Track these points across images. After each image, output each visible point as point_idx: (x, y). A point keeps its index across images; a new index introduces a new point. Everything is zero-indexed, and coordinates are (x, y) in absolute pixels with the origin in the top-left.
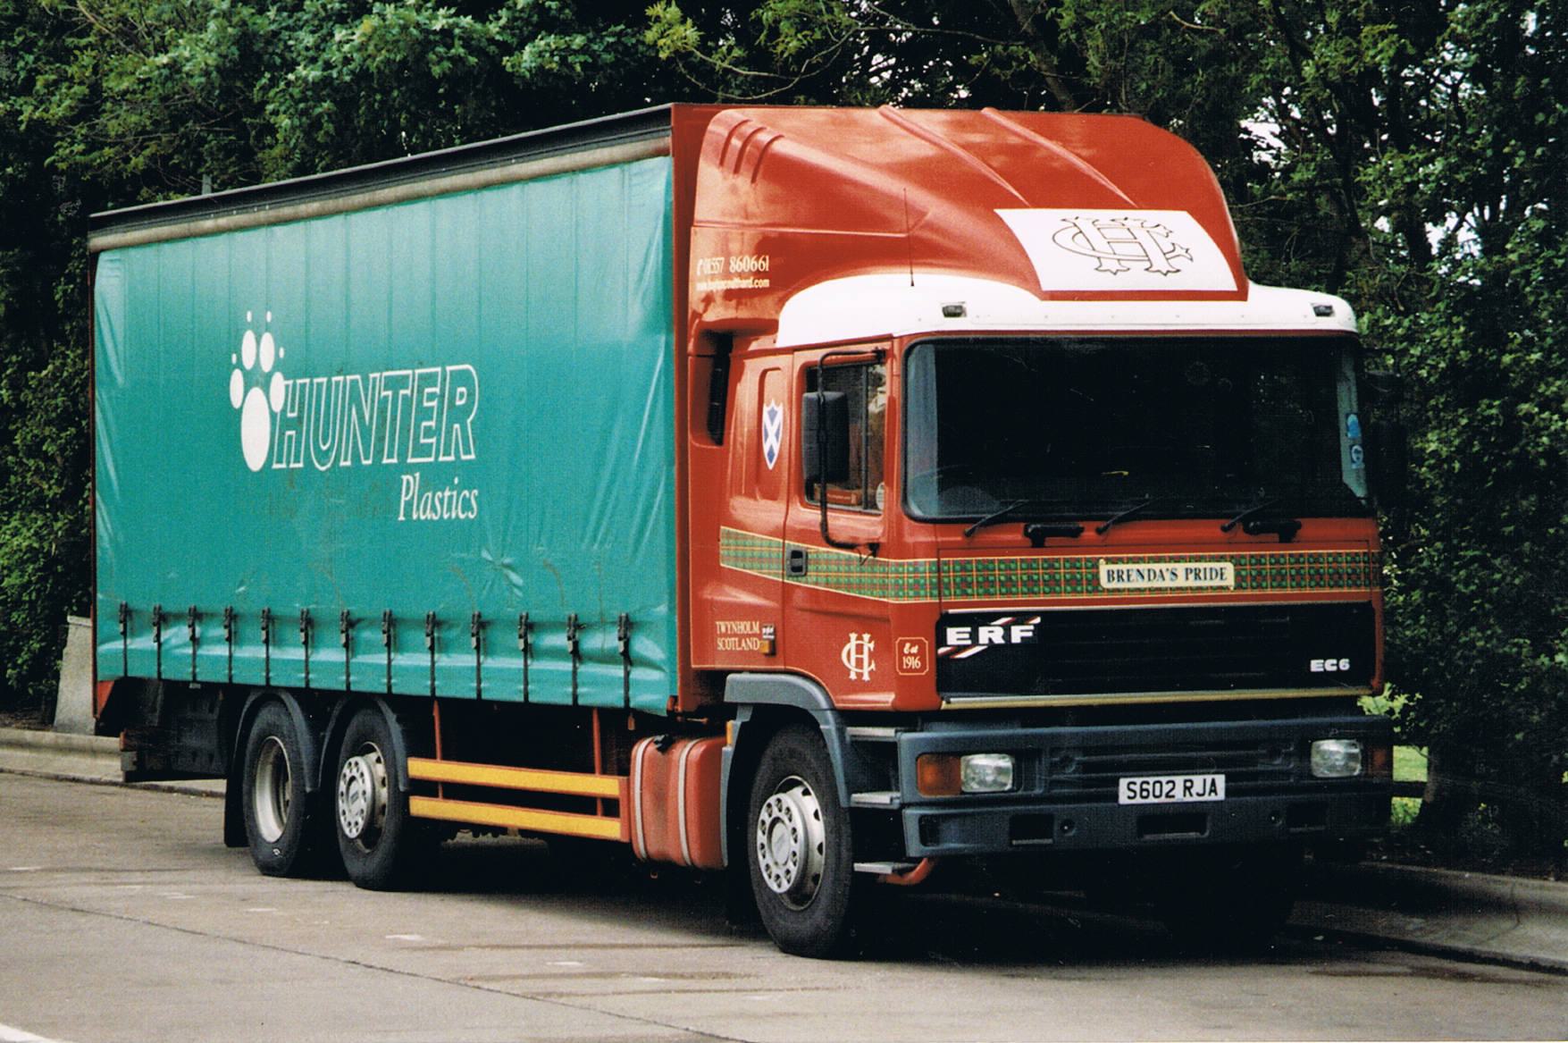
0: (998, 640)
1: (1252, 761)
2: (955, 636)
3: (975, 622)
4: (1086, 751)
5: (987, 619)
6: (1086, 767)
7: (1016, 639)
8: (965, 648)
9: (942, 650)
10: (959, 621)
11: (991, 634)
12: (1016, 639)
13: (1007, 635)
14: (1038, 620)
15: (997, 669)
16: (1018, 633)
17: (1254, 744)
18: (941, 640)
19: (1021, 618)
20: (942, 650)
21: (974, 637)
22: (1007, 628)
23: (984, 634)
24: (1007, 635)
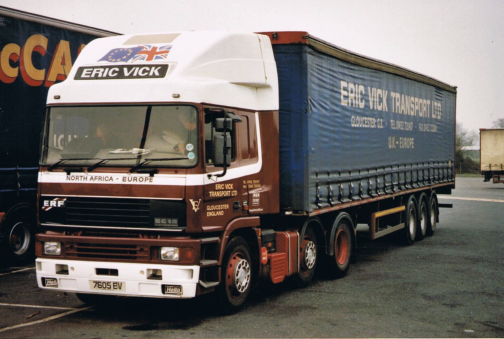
0: (55, 206)
1: (135, 252)
2: (46, 203)
3: (51, 199)
4: (79, 244)
5: (52, 198)
6: (79, 250)
8: (47, 207)
9: (43, 208)
11: (53, 203)
12: (59, 206)
13: (57, 204)
14: (65, 200)
15: (56, 214)
16: (60, 203)
17: (135, 246)
19: (61, 198)
21: (49, 203)
22: (57, 201)
24: (57, 204)
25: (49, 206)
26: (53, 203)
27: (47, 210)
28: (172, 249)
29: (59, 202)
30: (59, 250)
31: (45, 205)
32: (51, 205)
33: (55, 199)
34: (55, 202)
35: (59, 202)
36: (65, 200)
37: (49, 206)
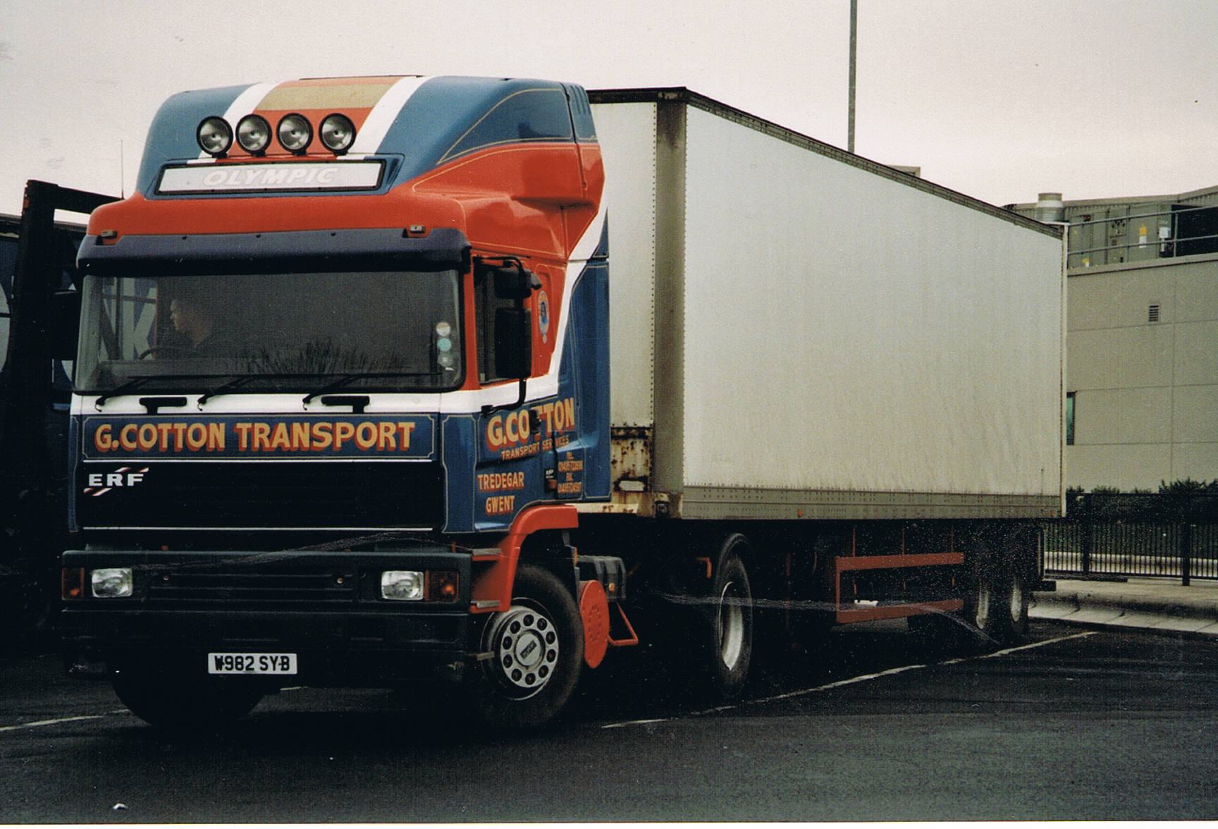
0: (119, 483)
2: (93, 480)
3: (107, 469)
5: (112, 468)
7: (131, 482)
8: (99, 489)
9: (86, 490)
10: (95, 468)
11: (115, 479)
12: (131, 482)
13: (125, 481)
14: (146, 470)
16: (132, 479)
19: (135, 468)
20: (86, 490)
21: (104, 480)
22: (125, 475)
23: (110, 476)
24: (125, 481)
25: (105, 486)
26: (115, 479)
27: (99, 494)
28: (406, 576)
30: (126, 589)
31: (92, 483)
32: (110, 483)
33: (122, 469)
34: (120, 477)
36: (146, 470)
37: (105, 486)
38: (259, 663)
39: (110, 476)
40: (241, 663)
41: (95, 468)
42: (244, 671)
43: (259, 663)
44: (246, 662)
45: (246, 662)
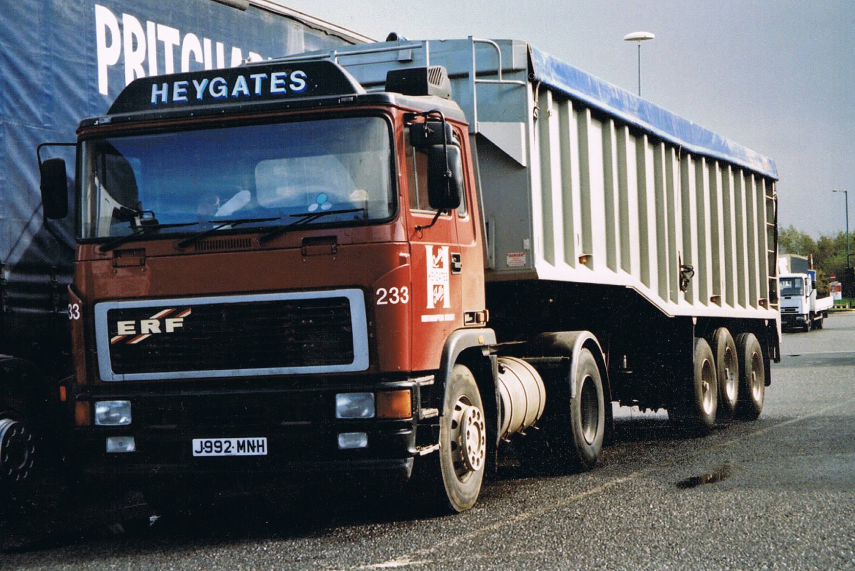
0: (156, 330)
10: (126, 314)
11: (151, 326)
13: (163, 326)
16: (171, 325)
18: (112, 330)
19: (176, 312)
21: (138, 327)
22: (162, 320)
23: (145, 326)
24: (163, 326)
26: (151, 326)
29: (167, 320)
34: (157, 323)
35: (167, 320)
38: (232, 447)
39: (144, 324)
40: (221, 447)
41: (126, 314)
42: (223, 454)
43: (232, 447)
44: (225, 446)
45: (225, 446)
